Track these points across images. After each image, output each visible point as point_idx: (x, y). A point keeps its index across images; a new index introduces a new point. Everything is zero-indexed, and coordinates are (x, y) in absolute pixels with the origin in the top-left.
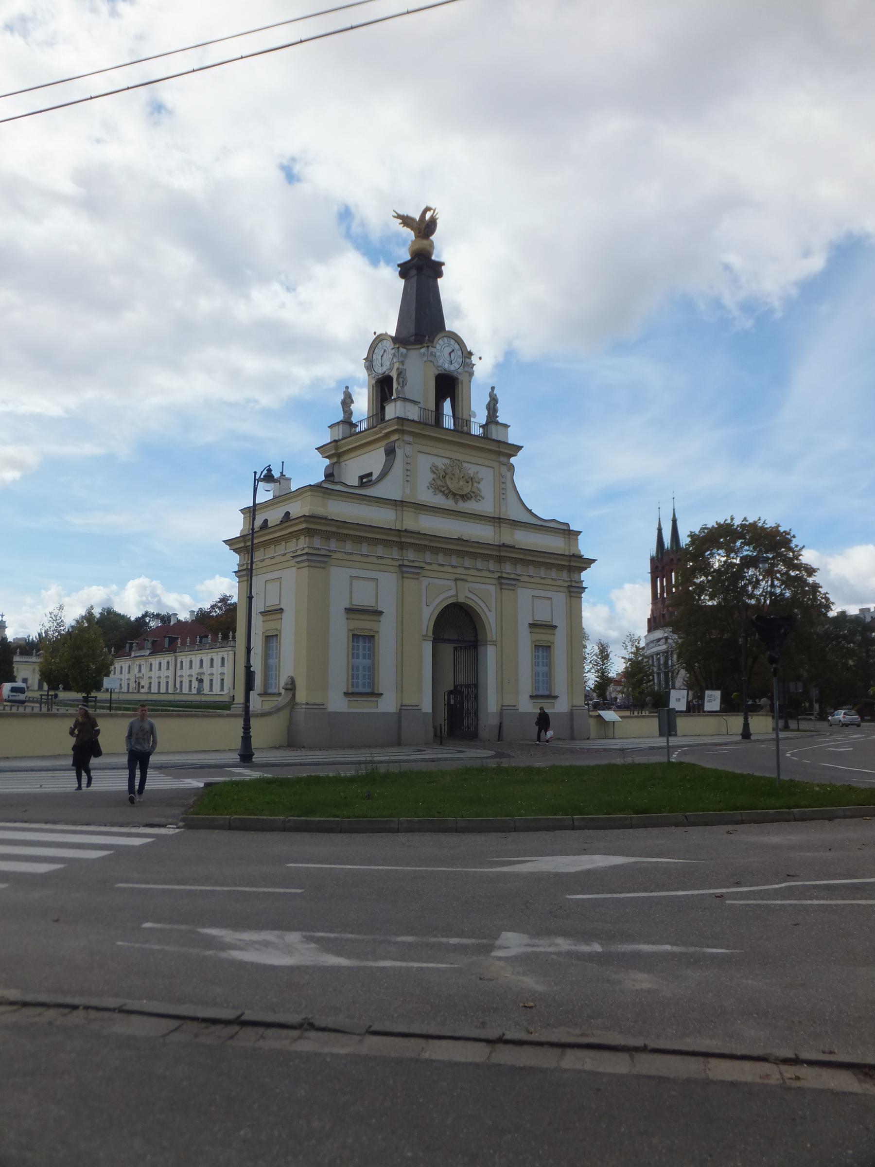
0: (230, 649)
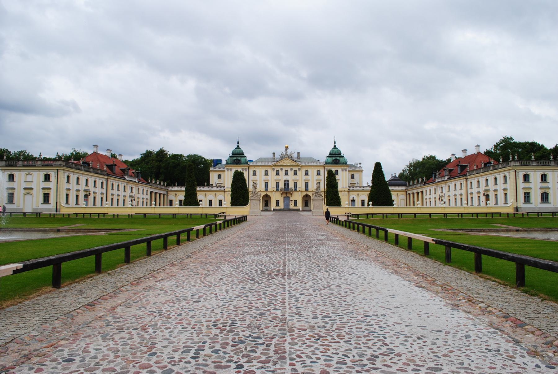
0: (511, 168)
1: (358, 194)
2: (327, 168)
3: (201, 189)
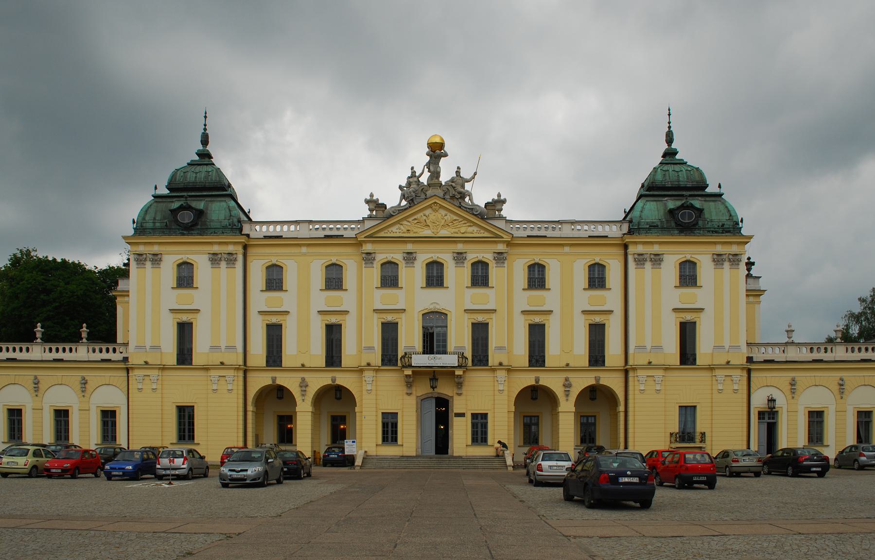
1: (793, 383)
2: (640, 249)
3: (18, 355)
